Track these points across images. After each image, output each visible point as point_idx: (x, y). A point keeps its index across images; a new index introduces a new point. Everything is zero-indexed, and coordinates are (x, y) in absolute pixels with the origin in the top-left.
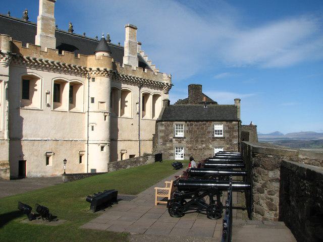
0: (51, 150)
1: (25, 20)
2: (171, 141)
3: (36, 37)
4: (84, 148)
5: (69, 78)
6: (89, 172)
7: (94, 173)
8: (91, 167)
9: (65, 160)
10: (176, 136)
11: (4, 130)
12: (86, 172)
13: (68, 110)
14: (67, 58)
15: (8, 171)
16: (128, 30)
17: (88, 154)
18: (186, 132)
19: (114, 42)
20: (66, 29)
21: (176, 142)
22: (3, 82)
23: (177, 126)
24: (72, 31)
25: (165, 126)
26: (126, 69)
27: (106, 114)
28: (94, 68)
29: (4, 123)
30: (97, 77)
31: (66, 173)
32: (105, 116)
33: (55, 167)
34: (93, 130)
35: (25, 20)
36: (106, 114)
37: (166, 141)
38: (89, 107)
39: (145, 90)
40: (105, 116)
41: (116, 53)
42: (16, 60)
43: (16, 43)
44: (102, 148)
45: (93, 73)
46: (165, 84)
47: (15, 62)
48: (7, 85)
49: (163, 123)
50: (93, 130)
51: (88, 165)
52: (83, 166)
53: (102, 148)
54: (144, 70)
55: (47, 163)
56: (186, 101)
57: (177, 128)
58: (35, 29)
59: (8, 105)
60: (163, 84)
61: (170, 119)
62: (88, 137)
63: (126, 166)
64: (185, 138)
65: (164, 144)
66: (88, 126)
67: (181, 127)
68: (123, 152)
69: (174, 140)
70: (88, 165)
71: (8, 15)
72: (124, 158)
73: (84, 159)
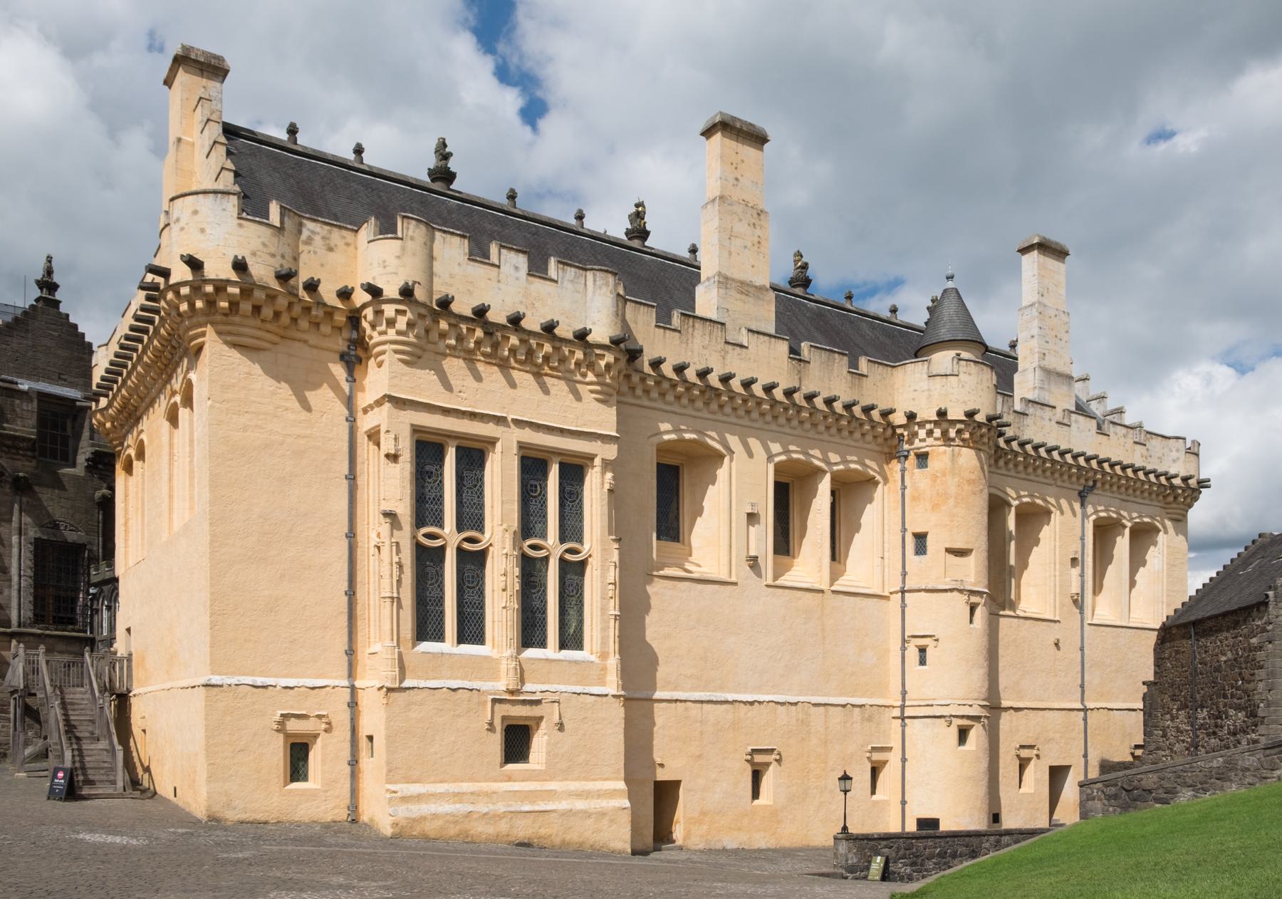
3: (700, 290)
5: (833, 460)
11: (604, 656)
14: (827, 377)
22: (597, 461)
27: (974, 599)
29: (605, 629)
31: (853, 830)
32: (973, 608)
34: (923, 662)
36: (974, 599)
38: (904, 574)
40: (973, 608)
44: (963, 734)
48: (609, 475)
50: (923, 662)
59: (616, 558)
62: (904, 693)
66: (904, 649)
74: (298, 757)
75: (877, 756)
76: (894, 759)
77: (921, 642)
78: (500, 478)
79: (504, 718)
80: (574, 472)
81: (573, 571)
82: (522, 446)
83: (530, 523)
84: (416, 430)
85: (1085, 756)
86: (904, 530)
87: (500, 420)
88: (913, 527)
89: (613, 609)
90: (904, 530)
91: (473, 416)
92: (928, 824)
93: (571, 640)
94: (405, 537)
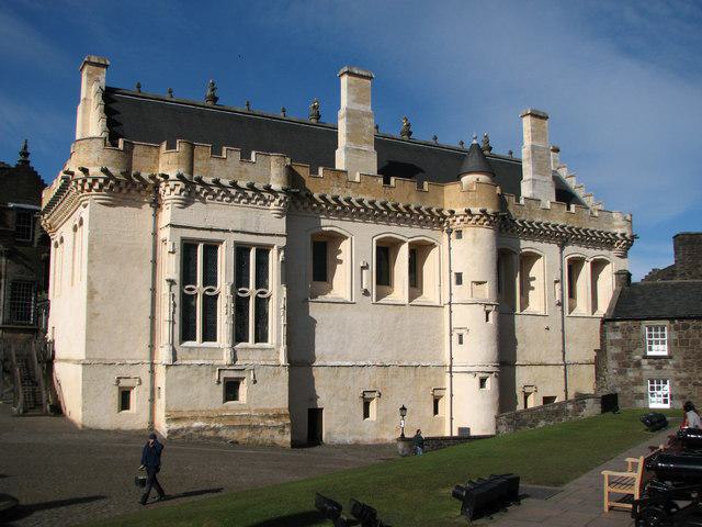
0: (374, 386)
1: (313, 121)
2: (638, 364)
4: (443, 382)
5: (408, 233)
6: (455, 434)
7: (465, 436)
8: (459, 423)
9: (403, 409)
10: (649, 353)
11: (279, 345)
12: (447, 434)
13: (406, 302)
15: (287, 430)
16: (527, 122)
17: (452, 395)
18: (672, 344)
19: (500, 150)
20: (396, 133)
21: (649, 367)
23: (650, 330)
24: (410, 133)
25: (622, 331)
26: (529, 206)
27: (488, 308)
28: (459, 210)
29: (278, 332)
32: (488, 313)
33: (382, 422)
34: (461, 342)
35: (313, 121)
36: (488, 308)
37: (626, 365)
38: (451, 294)
39: (572, 251)
40: (488, 313)
41: (505, 174)
42: (299, 203)
43: (296, 169)
44: (482, 382)
45: (458, 219)
46: (618, 235)
47: (297, 208)
48: (282, 254)
49: (618, 324)
50: (461, 342)
51: (452, 419)
52: (442, 421)
53: (482, 382)
54: (569, 208)
55: (366, 415)
56: (669, 273)
57: (650, 336)
58: (335, 136)
60: (614, 235)
61: (636, 314)
63: (536, 422)
64: (670, 357)
65: (622, 372)
66: (451, 335)
67: (659, 333)
69: (645, 362)
70: (452, 419)
71: (282, 114)
72: (531, 405)
73: (444, 405)
74: (125, 402)
75: (437, 393)
76: (447, 393)
79: (225, 378)
80: (263, 252)
81: (262, 304)
82: (236, 243)
84: (183, 239)
85: (566, 391)
86: (450, 271)
88: (456, 269)
89: (283, 321)
90: (450, 271)
91: (211, 230)
92: (464, 431)
93: (261, 336)
94: (176, 289)
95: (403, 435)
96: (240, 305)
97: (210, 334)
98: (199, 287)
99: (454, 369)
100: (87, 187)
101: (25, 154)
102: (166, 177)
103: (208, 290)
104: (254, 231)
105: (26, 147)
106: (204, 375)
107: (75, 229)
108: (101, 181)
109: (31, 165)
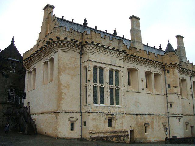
6: (171, 137)
28: (168, 64)
30: (171, 70)
34: (171, 107)
38: (166, 91)
50: (171, 107)
62: (168, 112)
66: (167, 104)
68: (187, 123)
77: (170, 103)
78: (106, 74)
83: (111, 82)
86: (166, 83)
87: (106, 64)
88: (167, 83)
90: (166, 83)
91: (102, 63)
95: (167, 137)
96: (111, 90)
97: (102, 102)
98: (99, 84)
99: (169, 116)
100: (58, 45)
101: (13, 41)
102: (87, 43)
103: (101, 85)
104: (114, 64)
105: (13, 39)
106: (102, 116)
107: (46, 63)
108: (65, 42)
109: (15, 46)
